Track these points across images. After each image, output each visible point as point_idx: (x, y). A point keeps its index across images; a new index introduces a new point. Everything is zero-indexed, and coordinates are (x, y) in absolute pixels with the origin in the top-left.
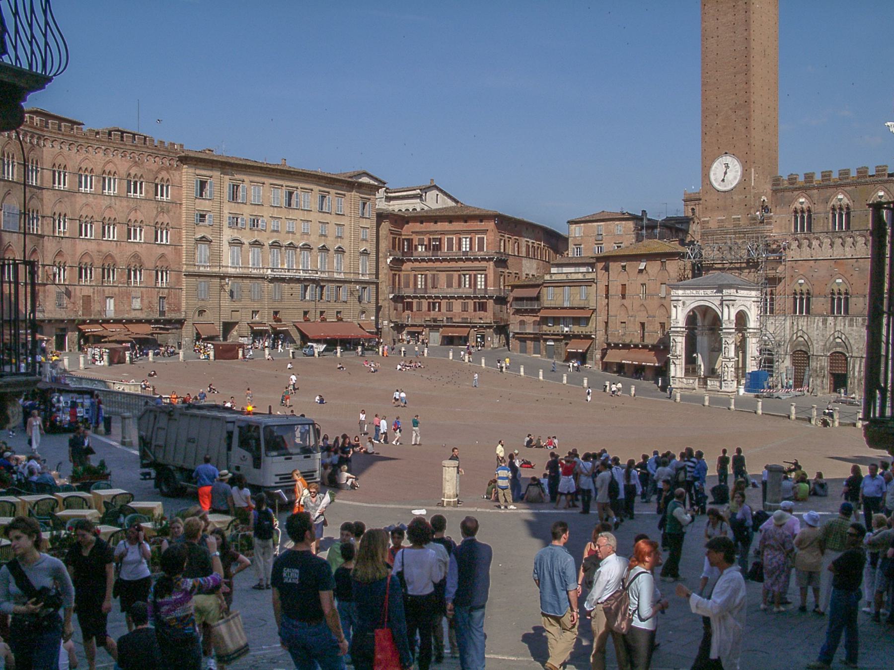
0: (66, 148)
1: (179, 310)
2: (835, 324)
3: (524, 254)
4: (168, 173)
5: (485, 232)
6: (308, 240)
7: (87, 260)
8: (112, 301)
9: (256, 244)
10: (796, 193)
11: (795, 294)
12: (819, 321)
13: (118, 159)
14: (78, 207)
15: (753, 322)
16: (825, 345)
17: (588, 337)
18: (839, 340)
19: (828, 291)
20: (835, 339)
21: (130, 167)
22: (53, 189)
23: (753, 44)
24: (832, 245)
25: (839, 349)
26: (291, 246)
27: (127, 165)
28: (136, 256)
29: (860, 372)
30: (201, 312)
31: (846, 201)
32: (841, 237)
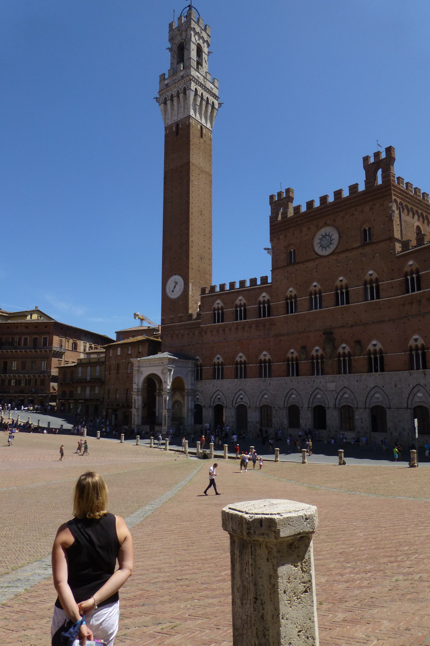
3: (82, 350)
5: (49, 333)
10: (215, 297)
15: (188, 386)
17: (98, 400)
23: (191, 205)
31: (244, 301)
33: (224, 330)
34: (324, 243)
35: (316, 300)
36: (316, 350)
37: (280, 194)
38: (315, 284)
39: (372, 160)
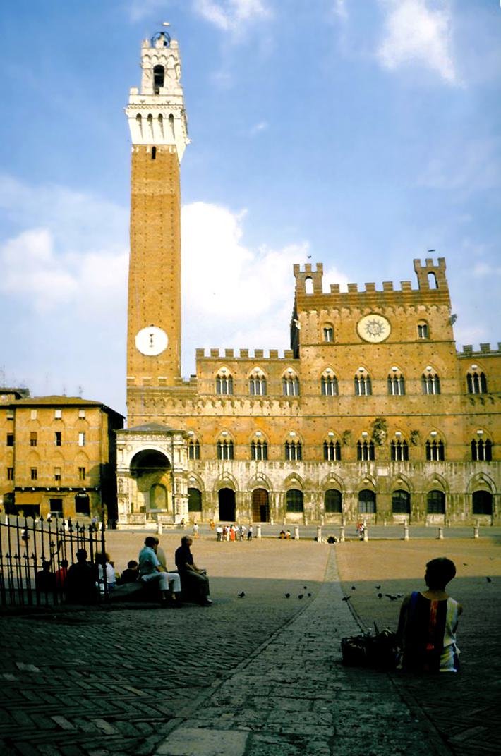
2: (257, 467)
10: (219, 363)
11: (219, 443)
12: (242, 464)
16: (249, 484)
18: (260, 480)
19: (250, 441)
20: (256, 478)
24: (252, 405)
25: (261, 487)
29: (280, 504)
31: (261, 373)
32: (259, 400)
33: (232, 404)
34: (372, 329)
35: (363, 383)
36: (365, 435)
37: (308, 266)
38: (362, 369)
39: (423, 264)
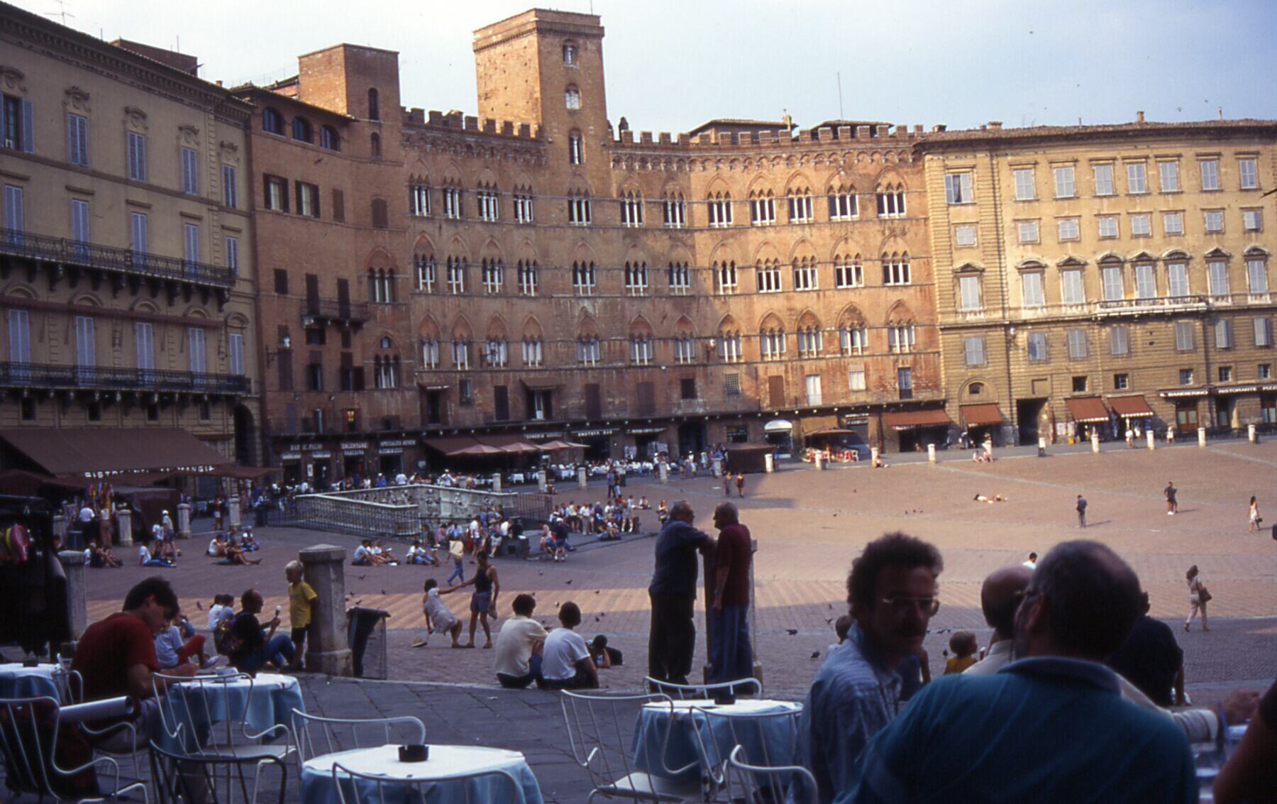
0: (725, 167)
1: (936, 386)
4: (898, 174)
6: (1181, 244)
7: (773, 324)
8: (818, 380)
9: (1070, 264)
13: (809, 169)
14: (751, 248)
21: (831, 177)
22: (711, 229)
26: (1143, 259)
27: (826, 174)
28: (852, 310)
30: (975, 389)
